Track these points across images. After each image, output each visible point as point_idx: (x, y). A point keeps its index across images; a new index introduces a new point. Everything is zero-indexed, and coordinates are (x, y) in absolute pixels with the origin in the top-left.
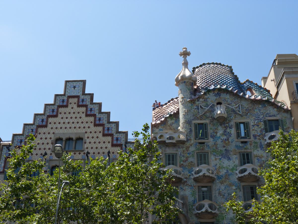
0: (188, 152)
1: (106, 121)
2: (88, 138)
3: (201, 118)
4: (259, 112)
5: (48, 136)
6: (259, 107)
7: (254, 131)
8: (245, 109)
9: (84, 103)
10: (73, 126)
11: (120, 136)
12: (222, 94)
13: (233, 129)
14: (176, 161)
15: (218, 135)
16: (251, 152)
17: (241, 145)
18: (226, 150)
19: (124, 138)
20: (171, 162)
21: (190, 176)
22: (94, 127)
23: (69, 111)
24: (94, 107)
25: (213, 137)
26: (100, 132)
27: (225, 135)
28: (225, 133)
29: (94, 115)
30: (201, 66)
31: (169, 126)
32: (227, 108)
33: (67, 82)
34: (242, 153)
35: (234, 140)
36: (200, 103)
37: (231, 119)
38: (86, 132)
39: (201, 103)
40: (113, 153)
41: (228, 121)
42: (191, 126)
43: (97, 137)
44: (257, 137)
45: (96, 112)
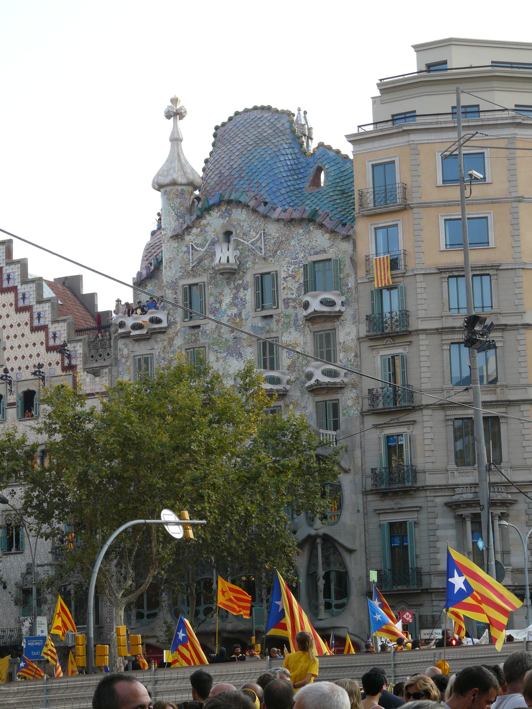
2: (8, 337)
3: (195, 271)
4: (297, 245)
6: (298, 232)
7: (286, 291)
8: (272, 241)
12: (234, 210)
13: (249, 290)
15: (224, 306)
16: (278, 337)
17: (260, 325)
19: (66, 331)
22: (15, 315)
24: (14, 270)
26: (26, 324)
27: (236, 305)
29: (14, 289)
30: (230, 119)
32: (238, 243)
34: (261, 341)
35: (250, 316)
36: (192, 239)
37: (247, 269)
38: (4, 327)
39: (195, 237)
40: (50, 364)
41: (241, 273)
42: (176, 293)
43: (23, 335)
44: (291, 304)
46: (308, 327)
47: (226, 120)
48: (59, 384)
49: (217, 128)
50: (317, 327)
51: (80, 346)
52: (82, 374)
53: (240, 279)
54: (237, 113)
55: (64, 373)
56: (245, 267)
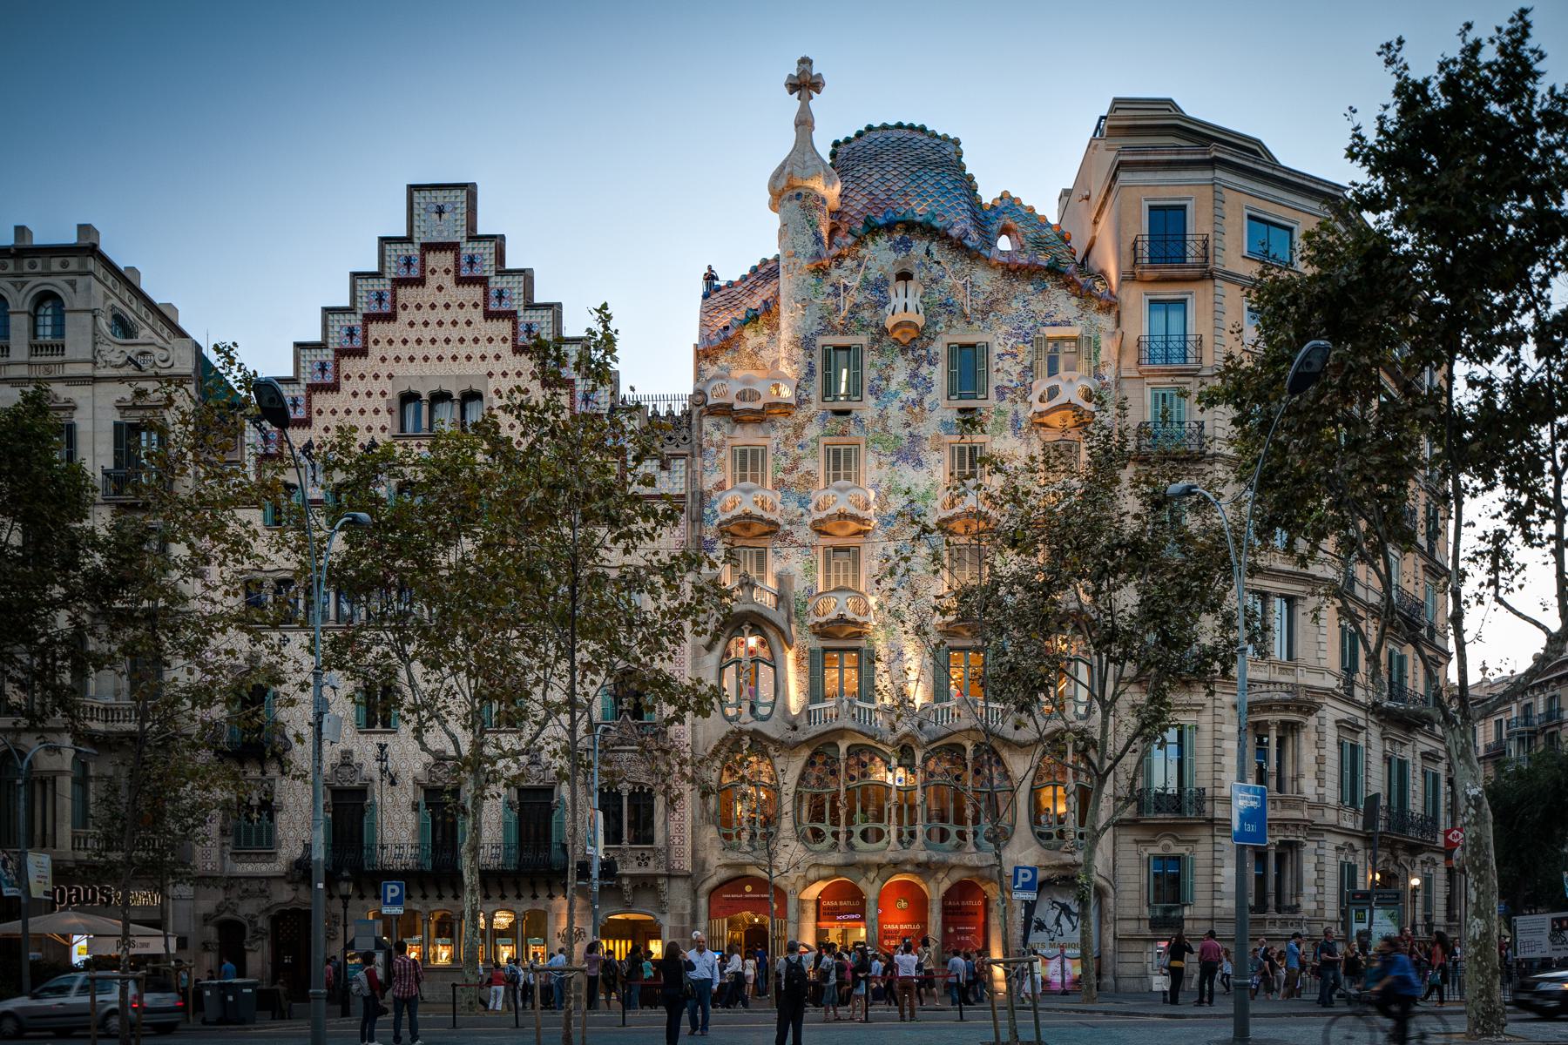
5: (376, 387)
7: (1001, 375)
9: (477, 273)
10: (448, 351)
12: (915, 242)
13: (939, 365)
15: (893, 386)
18: (911, 435)
20: (749, 473)
23: (432, 299)
25: (875, 392)
27: (915, 387)
28: (914, 379)
33: (413, 189)
37: (937, 334)
38: (490, 375)
45: (517, 304)
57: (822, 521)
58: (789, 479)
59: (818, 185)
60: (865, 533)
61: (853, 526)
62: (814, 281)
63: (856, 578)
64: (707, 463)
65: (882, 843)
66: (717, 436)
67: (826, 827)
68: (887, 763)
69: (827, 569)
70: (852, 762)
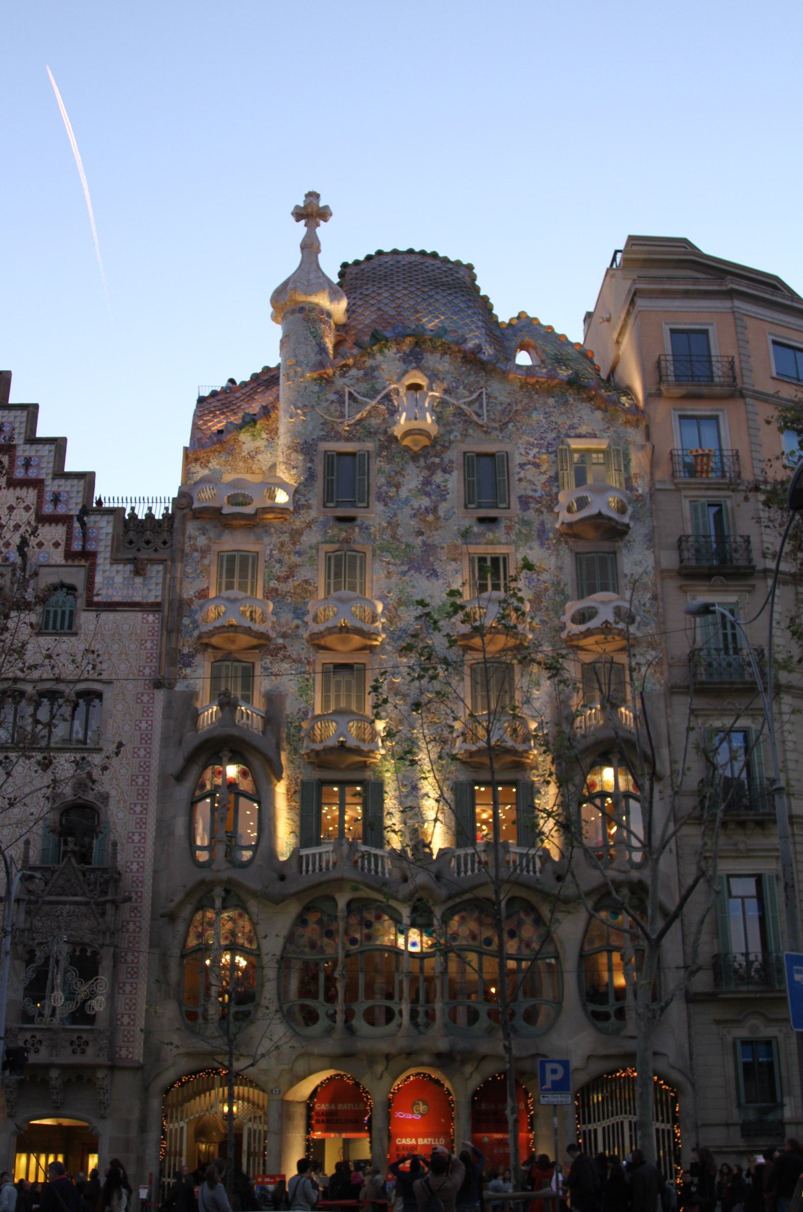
0: (298, 548)
1: (23, 436)
6: (545, 403)
7: (524, 484)
8: (499, 408)
11: (68, 489)
13: (455, 473)
14: (253, 577)
15: (404, 493)
18: (424, 543)
19: (81, 494)
20: (236, 580)
21: (297, 627)
27: (428, 495)
30: (369, 258)
31: (245, 460)
37: (451, 442)
39: (353, 382)
41: (438, 448)
42: (312, 461)
46: (566, 543)
47: (362, 258)
48: (54, 579)
49: (345, 265)
50: (582, 546)
51: (108, 522)
52: (108, 567)
53: (435, 456)
54: (380, 253)
55: (70, 562)
56: (446, 438)
57: (321, 635)
58: (282, 587)
59: (322, 300)
60: (372, 648)
61: (357, 640)
62: (316, 389)
63: (361, 701)
64: (189, 570)
65: (393, 1025)
66: (202, 541)
67: (320, 1006)
68: (397, 920)
69: (326, 689)
70: (354, 920)
